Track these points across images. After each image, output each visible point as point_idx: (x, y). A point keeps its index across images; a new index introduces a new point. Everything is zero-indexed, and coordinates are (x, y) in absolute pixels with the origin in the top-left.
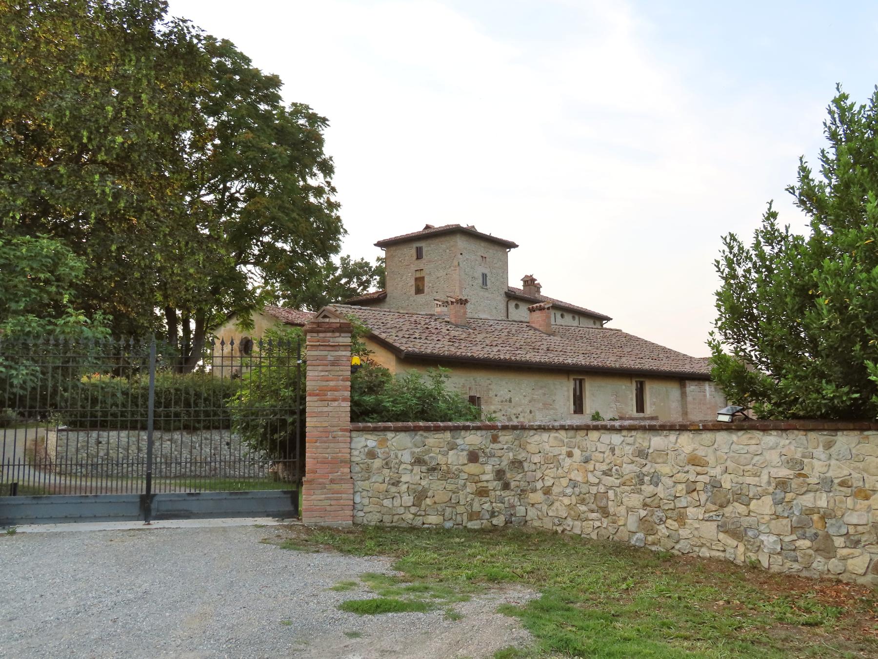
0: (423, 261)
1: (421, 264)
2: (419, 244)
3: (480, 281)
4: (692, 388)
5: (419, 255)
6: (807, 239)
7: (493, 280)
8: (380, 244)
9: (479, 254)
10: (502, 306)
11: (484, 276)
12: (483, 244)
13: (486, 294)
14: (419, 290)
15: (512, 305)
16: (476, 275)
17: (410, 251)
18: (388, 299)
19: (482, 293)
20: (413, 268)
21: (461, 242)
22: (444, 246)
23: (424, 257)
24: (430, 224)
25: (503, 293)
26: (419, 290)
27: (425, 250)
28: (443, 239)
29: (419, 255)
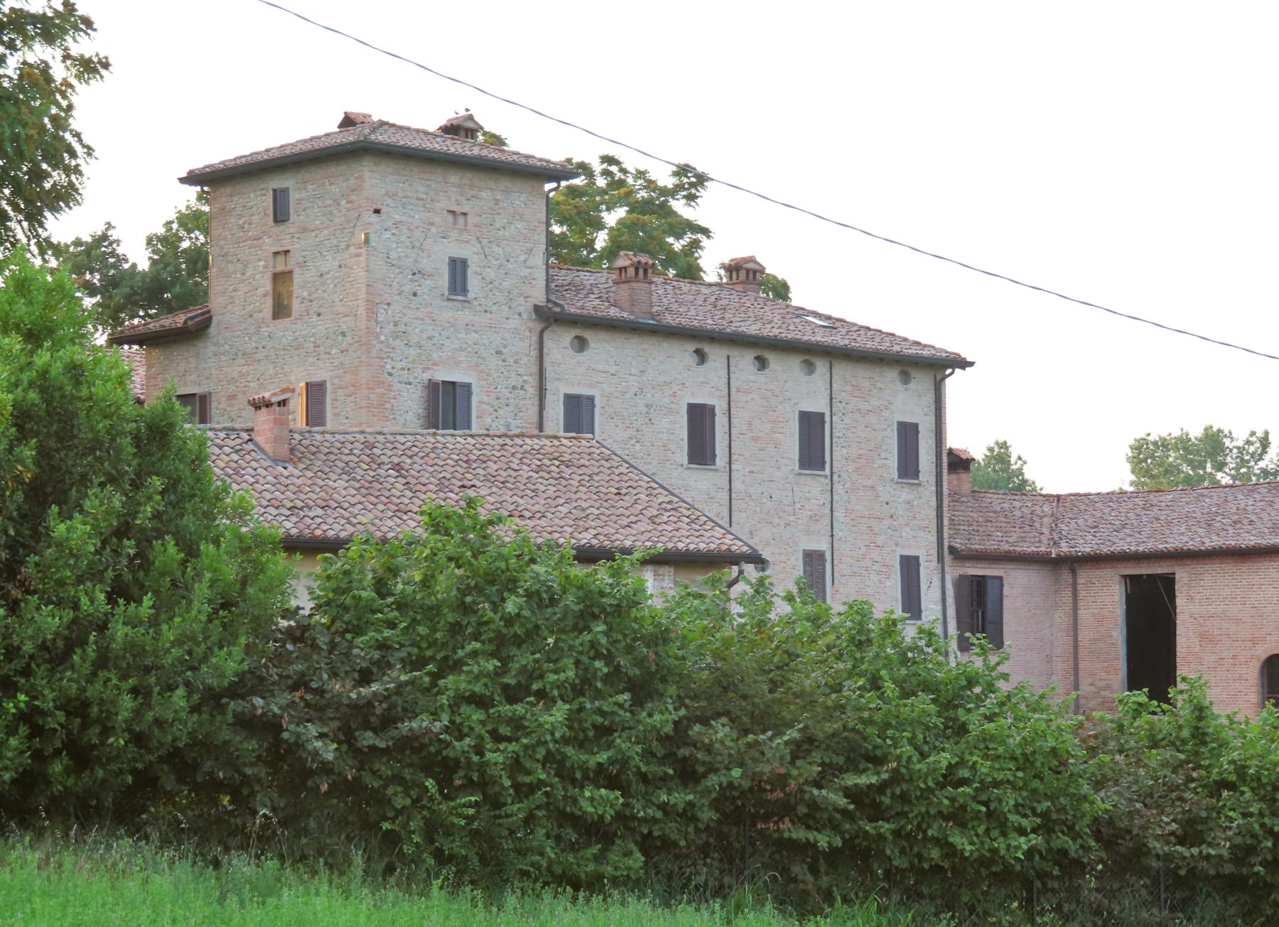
0: (290, 228)
1: (284, 237)
2: (277, 182)
3: (444, 281)
4: (1084, 576)
5: (280, 215)
6: (604, 214)
7: (490, 273)
8: (192, 178)
9: (443, 204)
10: (523, 346)
11: (458, 269)
12: (454, 177)
13: (466, 316)
14: (280, 309)
15: (559, 344)
16: (426, 265)
17: (258, 199)
18: (213, 330)
19: (449, 313)
20: (269, 245)
21: (374, 180)
22: (335, 189)
23: (293, 217)
24: (356, 108)
25: (526, 308)
26: (280, 309)
27: (294, 196)
28: (333, 169)
29: (280, 215)
